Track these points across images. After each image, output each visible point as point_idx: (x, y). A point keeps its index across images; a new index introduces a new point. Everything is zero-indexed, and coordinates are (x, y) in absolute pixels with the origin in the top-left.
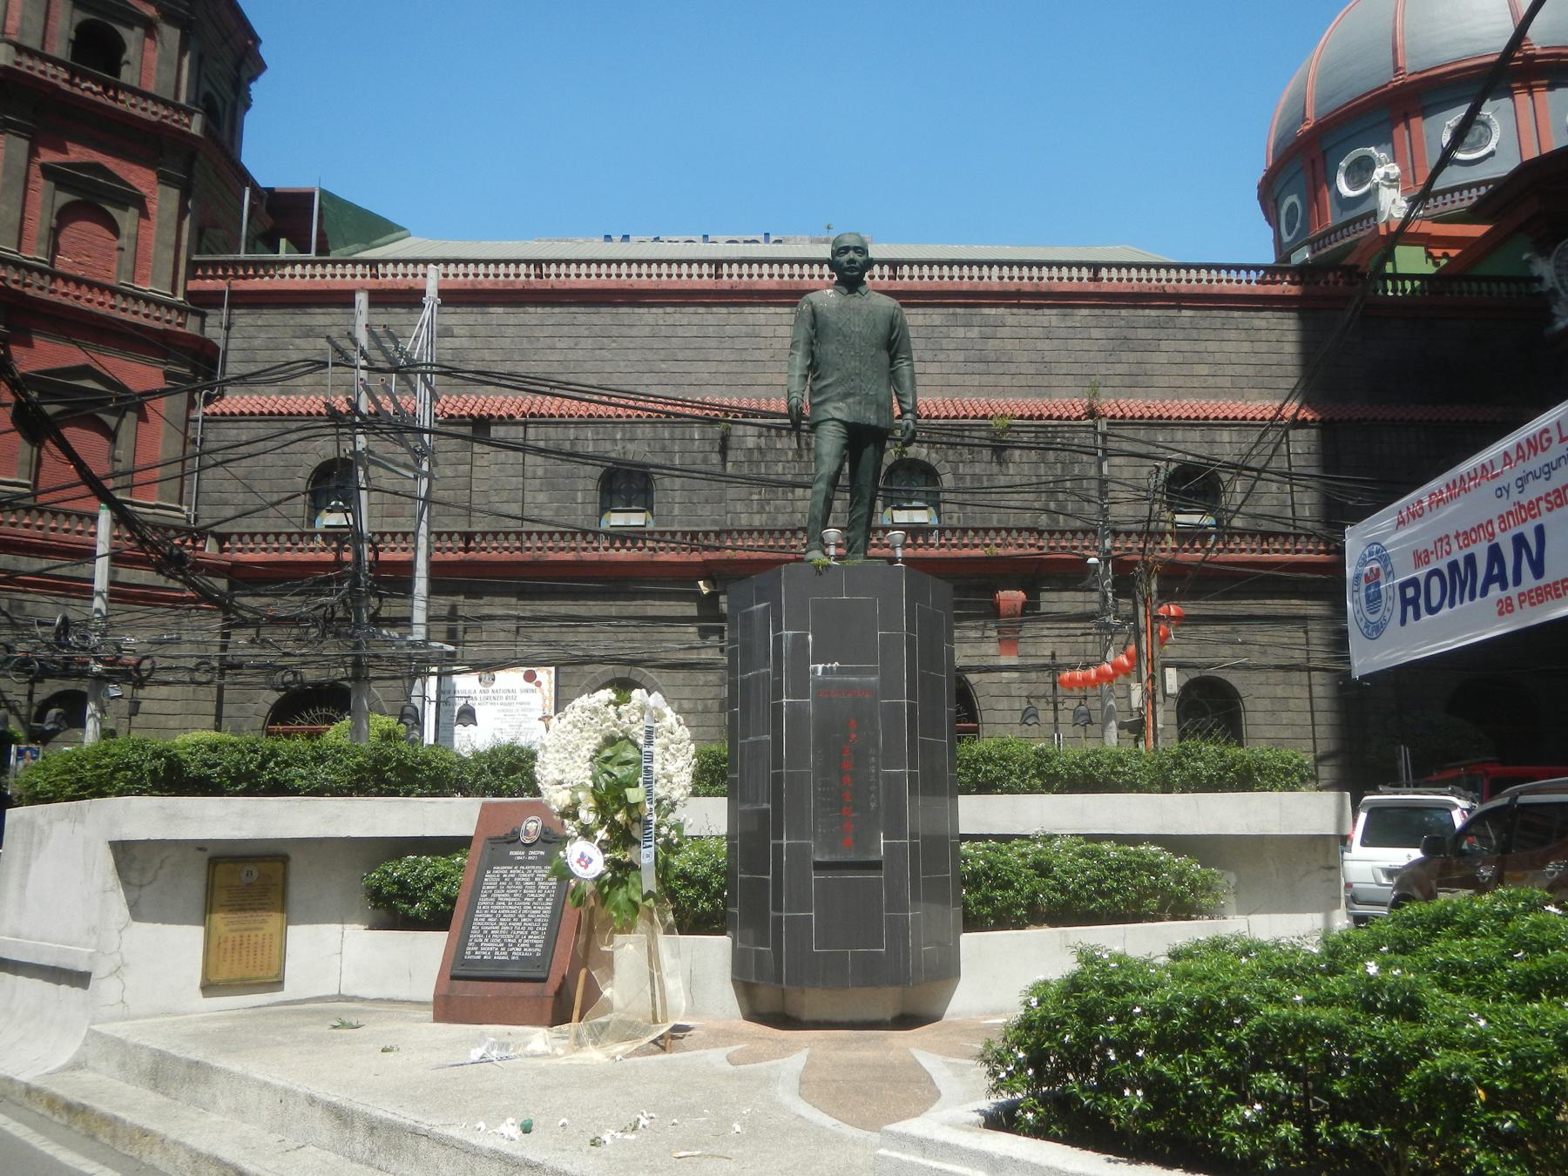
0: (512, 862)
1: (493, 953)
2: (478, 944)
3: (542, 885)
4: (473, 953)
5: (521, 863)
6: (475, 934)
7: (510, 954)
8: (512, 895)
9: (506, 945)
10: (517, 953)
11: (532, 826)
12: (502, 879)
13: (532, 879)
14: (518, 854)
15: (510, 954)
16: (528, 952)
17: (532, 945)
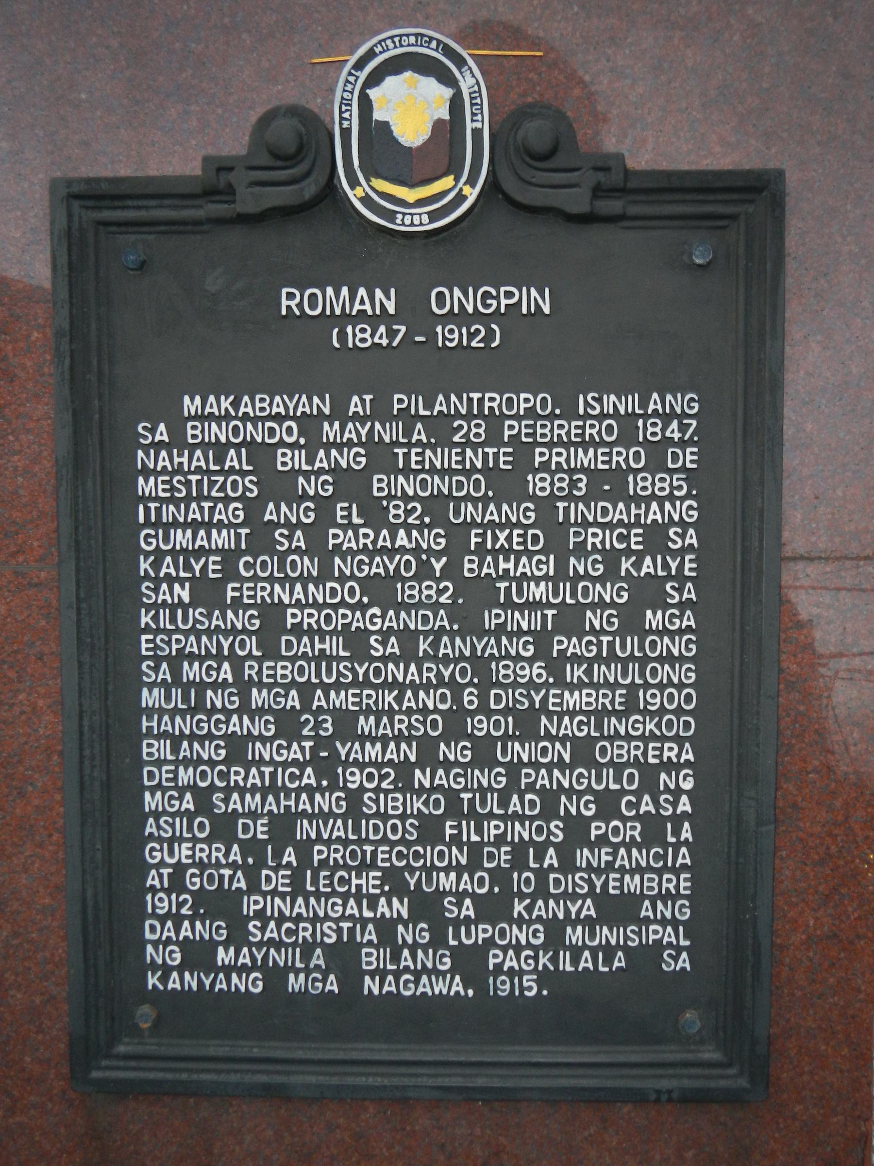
0: (307, 359)
1: (344, 957)
2: (219, 904)
3: (600, 526)
4: (198, 955)
5: (377, 373)
6: (174, 847)
7: (470, 963)
8: (380, 591)
9: (426, 907)
10: (518, 963)
11: (410, 108)
12: (279, 486)
13: (506, 485)
14: (359, 310)
15: (470, 963)
16: (594, 949)
17: (618, 909)
